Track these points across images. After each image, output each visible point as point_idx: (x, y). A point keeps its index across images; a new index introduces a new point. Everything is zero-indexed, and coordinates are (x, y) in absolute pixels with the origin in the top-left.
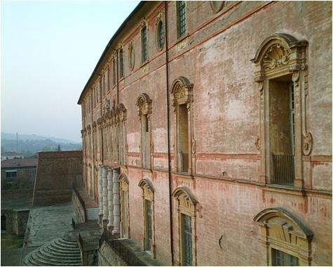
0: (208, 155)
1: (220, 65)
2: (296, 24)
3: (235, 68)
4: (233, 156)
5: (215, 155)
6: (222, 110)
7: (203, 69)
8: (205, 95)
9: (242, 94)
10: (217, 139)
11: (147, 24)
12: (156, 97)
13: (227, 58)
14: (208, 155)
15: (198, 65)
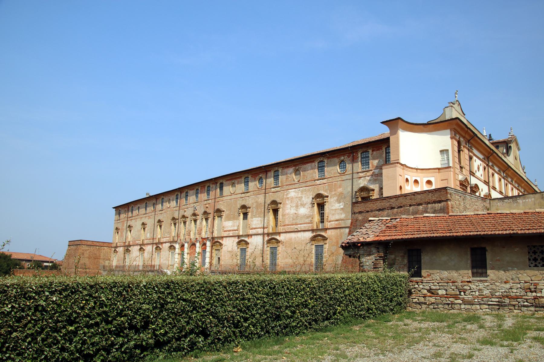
0: (288, 225)
1: (296, 197)
2: (326, 191)
3: (303, 199)
4: (301, 224)
5: (292, 225)
6: (297, 211)
7: (288, 198)
8: (288, 206)
9: (306, 206)
10: (293, 219)
11: (250, 177)
12: (254, 206)
13: (300, 196)
14: (288, 225)
15: (285, 196)
